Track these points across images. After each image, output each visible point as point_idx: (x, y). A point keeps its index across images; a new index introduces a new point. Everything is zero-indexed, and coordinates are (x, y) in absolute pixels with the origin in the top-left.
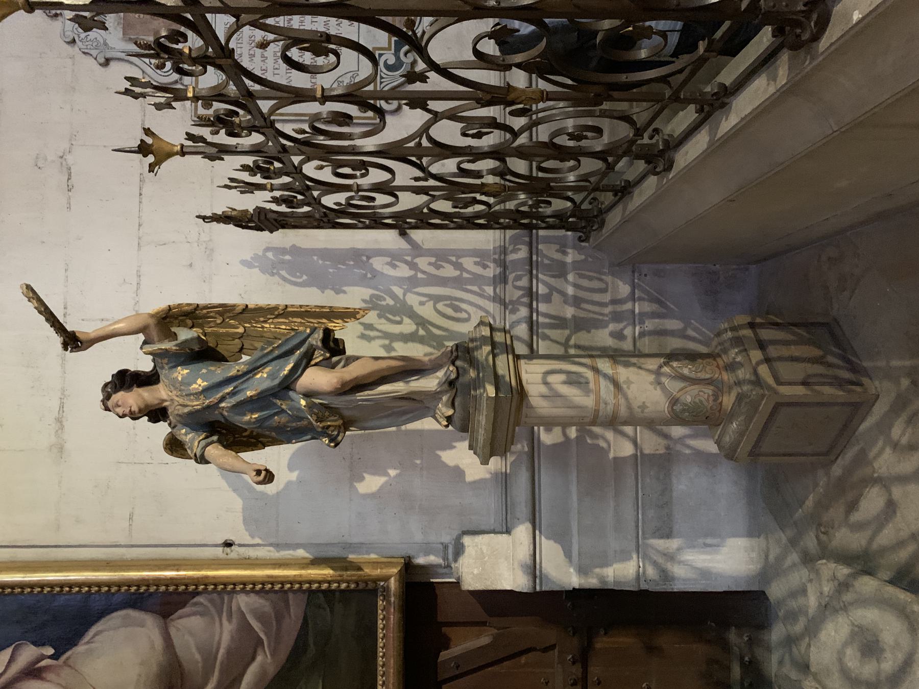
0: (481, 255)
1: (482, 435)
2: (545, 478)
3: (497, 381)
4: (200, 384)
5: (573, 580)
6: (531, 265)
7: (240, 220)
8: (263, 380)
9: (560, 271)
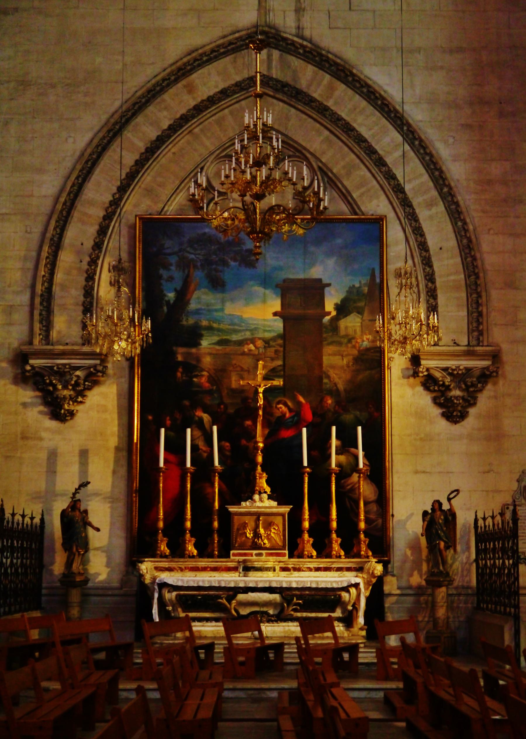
0: (470, 581)
1: (431, 578)
2: (411, 599)
3: (443, 581)
4: (441, 521)
5: (387, 605)
6: (467, 595)
7: (476, 520)
9: (466, 602)
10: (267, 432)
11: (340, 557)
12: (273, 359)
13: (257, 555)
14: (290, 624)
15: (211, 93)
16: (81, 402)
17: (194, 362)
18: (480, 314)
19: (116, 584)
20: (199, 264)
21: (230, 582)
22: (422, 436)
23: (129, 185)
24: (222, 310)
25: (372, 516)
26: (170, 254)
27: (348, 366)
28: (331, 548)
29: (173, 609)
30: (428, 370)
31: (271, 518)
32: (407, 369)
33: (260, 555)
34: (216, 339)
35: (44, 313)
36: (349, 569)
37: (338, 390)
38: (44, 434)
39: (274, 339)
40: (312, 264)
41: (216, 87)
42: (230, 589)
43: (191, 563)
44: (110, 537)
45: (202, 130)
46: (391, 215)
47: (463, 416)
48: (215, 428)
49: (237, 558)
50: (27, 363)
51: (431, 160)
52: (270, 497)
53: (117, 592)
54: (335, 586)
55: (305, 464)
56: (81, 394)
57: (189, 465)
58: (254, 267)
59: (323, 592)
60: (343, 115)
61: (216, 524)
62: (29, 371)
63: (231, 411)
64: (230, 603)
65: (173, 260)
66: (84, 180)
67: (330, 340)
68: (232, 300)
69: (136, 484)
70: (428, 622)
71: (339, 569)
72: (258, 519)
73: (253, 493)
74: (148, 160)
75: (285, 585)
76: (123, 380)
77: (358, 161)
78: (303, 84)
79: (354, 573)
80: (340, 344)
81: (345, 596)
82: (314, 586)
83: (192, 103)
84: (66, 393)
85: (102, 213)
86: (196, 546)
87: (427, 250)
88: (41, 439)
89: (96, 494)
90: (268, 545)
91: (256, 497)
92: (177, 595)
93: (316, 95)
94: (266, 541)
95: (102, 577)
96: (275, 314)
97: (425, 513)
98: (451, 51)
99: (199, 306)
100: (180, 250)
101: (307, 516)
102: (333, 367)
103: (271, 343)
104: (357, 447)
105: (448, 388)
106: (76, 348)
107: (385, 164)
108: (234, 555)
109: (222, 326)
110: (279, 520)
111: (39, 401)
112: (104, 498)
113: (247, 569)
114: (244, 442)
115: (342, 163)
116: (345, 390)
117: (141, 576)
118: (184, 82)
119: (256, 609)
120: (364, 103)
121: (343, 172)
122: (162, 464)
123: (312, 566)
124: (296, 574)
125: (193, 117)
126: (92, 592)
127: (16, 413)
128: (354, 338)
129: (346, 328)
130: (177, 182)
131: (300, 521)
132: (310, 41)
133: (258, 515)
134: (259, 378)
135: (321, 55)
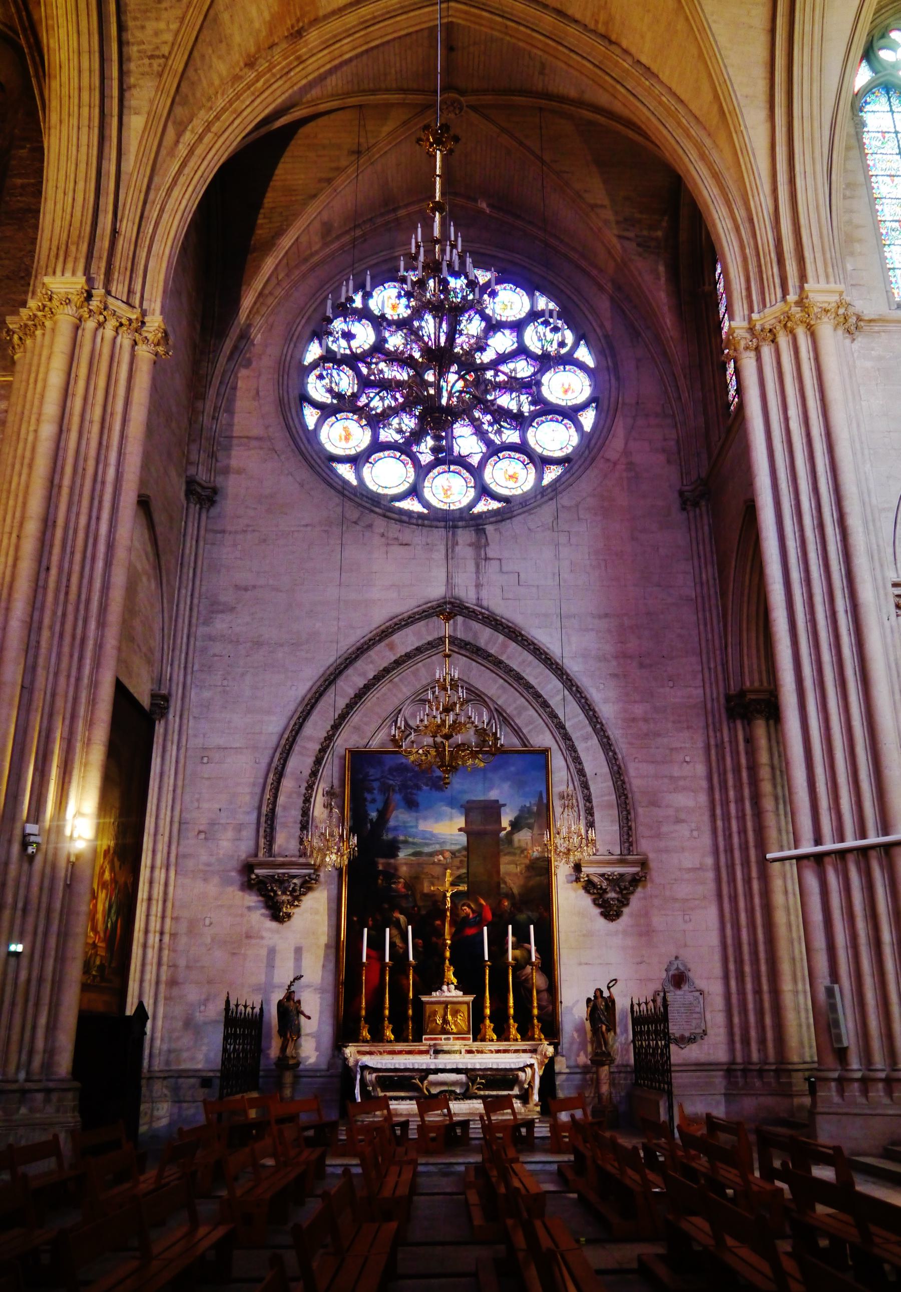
0: (628, 1060)
1: (596, 1058)
2: (578, 1076)
5: (557, 1083)
7: (632, 1006)
8: (604, 1019)
10: (453, 930)
11: (516, 1040)
12: (458, 868)
13: (445, 1039)
14: (475, 1101)
15: (408, 650)
16: (297, 906)
17: (392, 871)
18: (630, 828)
19: (324, 1066)
20: (397, 788)
21: (422, 1064)
22: (585, 932)
23: (340, 724)
24: (416, 827)
25: (544, 1003)
26: (373, 781)
27: (521, 873)
28: (509, 1032)
29: (373, 1089)
30: (588, 876)
31: (458, 1007)
32: (571, 875)
33: (448, 1039)
34: (410, 851)
35: (268, 830)
36: (524, 1051)
37: (513, 893)
38: (265, 934)
39: (459, 851)
40: (491, 788)
41: (412, 645)
42: (423, 1070)
43: (389, 1047)
44: (319, 1024)
45: (401, 680)
46: (554, 747)
47: (618, 915)
48: (410, 927)
49: (428, 1042)
50: (253, 872)
51: (586, 702)
52: (456, 988)
53: (323, 1073)
54: (513, 1066)
55: (486, 958)
56: (297, 898)
57: (387, 960)
58: (443, 791)
59: (502, 1073)
60: (515, 667)
61: (410, 1012)
62: (254, 879)
63: (423, 912)
64: (422, 1083)
65: (376, 785)
66: (304, 720)
67: (507, 851)
68: (425, 818)
69: (343, 977)
70: (594, 1098)
71: (516, 1051)
72: (446, 1008)
73: (442, 984)
74: (356, 703)
75: (469, 1067)
76: (333, 886)
77: (527, 703)
78: (482, 643)
79: (529, 1055)
80: (514, 854)
81: (521, 1075)
82: (495, 1067)
83: (393, 658)
84: (284, 898)
85: (318, 747)
86: (393, 1032)
87: (585, 776)
88: (262, 938)
89: (308, 986)
90: (455, 1030)
91: (445, 988)
92: (376, 1077)
93: (492, 651)
94: (453, 1027)
95: (312, 1060)
96: (460, 830)
97: (589, 1000)
98: (600, 617)
99: (396, 824)
100: (382, 777)
101: (488, 1004)
102: (509, 874)
103: (457, 854)
104: (529, 943)
105: (605, 891)
106: (293, 859)
107: (548, 706)
108: (426, 1039)
109: (416, 840)
110: (464, 1008)
111: (262, 905)
112: (315, 989)
113: (437, 1052)
114: (434, 939)
115: (515, 705)
116: (519, 894)
117: (346, 1059)
118: (387, 641)
119: (445, 1088)
120: (531, 658)
121: (515, 713)
122: (364, 960)
123: (493, 1048)
124: (479, 1055)
125: (394, 669)
126: (302, 1074)
127: (242, 915)
128: (526, 849)
129: (519, 840)
130: (380, 722)
131: (483, 1008)
132: (488, 610)
133: (446, 1004)
134: (447, 884)
135: (497, 620)
